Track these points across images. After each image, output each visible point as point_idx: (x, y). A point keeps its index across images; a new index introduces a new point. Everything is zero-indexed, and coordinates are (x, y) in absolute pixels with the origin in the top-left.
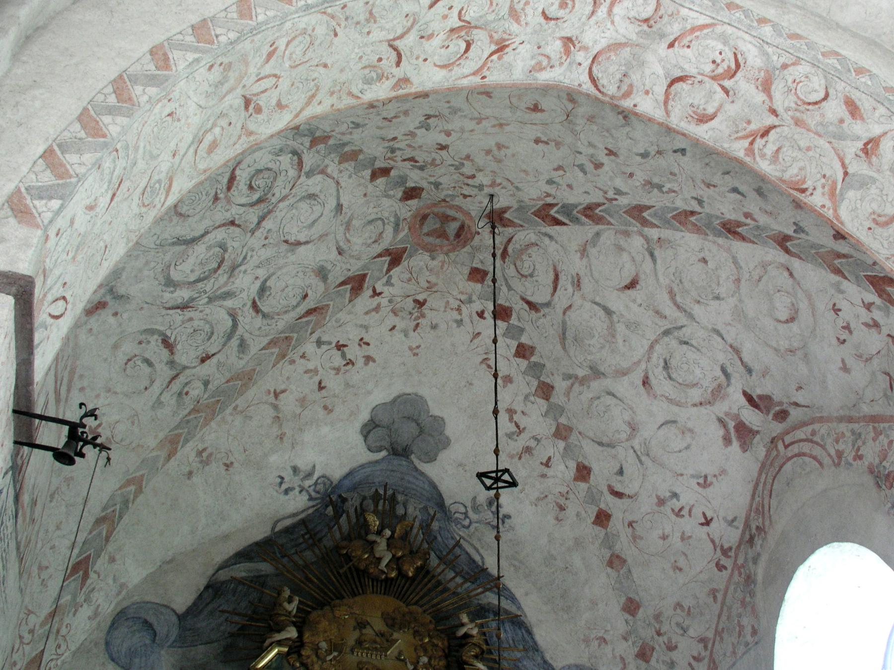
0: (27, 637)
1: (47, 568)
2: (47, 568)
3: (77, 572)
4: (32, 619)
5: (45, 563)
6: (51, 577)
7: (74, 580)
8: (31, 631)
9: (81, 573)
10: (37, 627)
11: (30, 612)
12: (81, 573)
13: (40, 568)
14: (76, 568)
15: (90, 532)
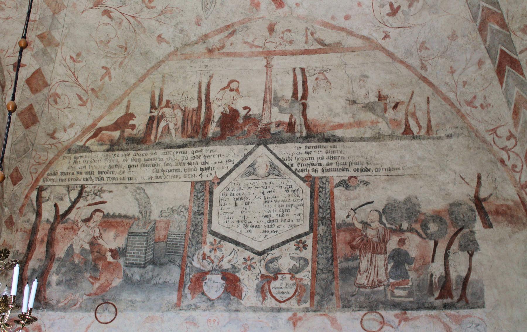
0: (510, 144)
1: (475, 97)
2: (475, 97)
3: (505, 71)
4: (503, 132)
5: (469, 98)
6: (485, 97)
7: (507, 77)
8: (511, 136)
9: (508, 68)
10: (513, 131)
11: (494, 131)
12: (508, 68)
13: (469, 103)
14: (500, 72)
15: (485, 41)
